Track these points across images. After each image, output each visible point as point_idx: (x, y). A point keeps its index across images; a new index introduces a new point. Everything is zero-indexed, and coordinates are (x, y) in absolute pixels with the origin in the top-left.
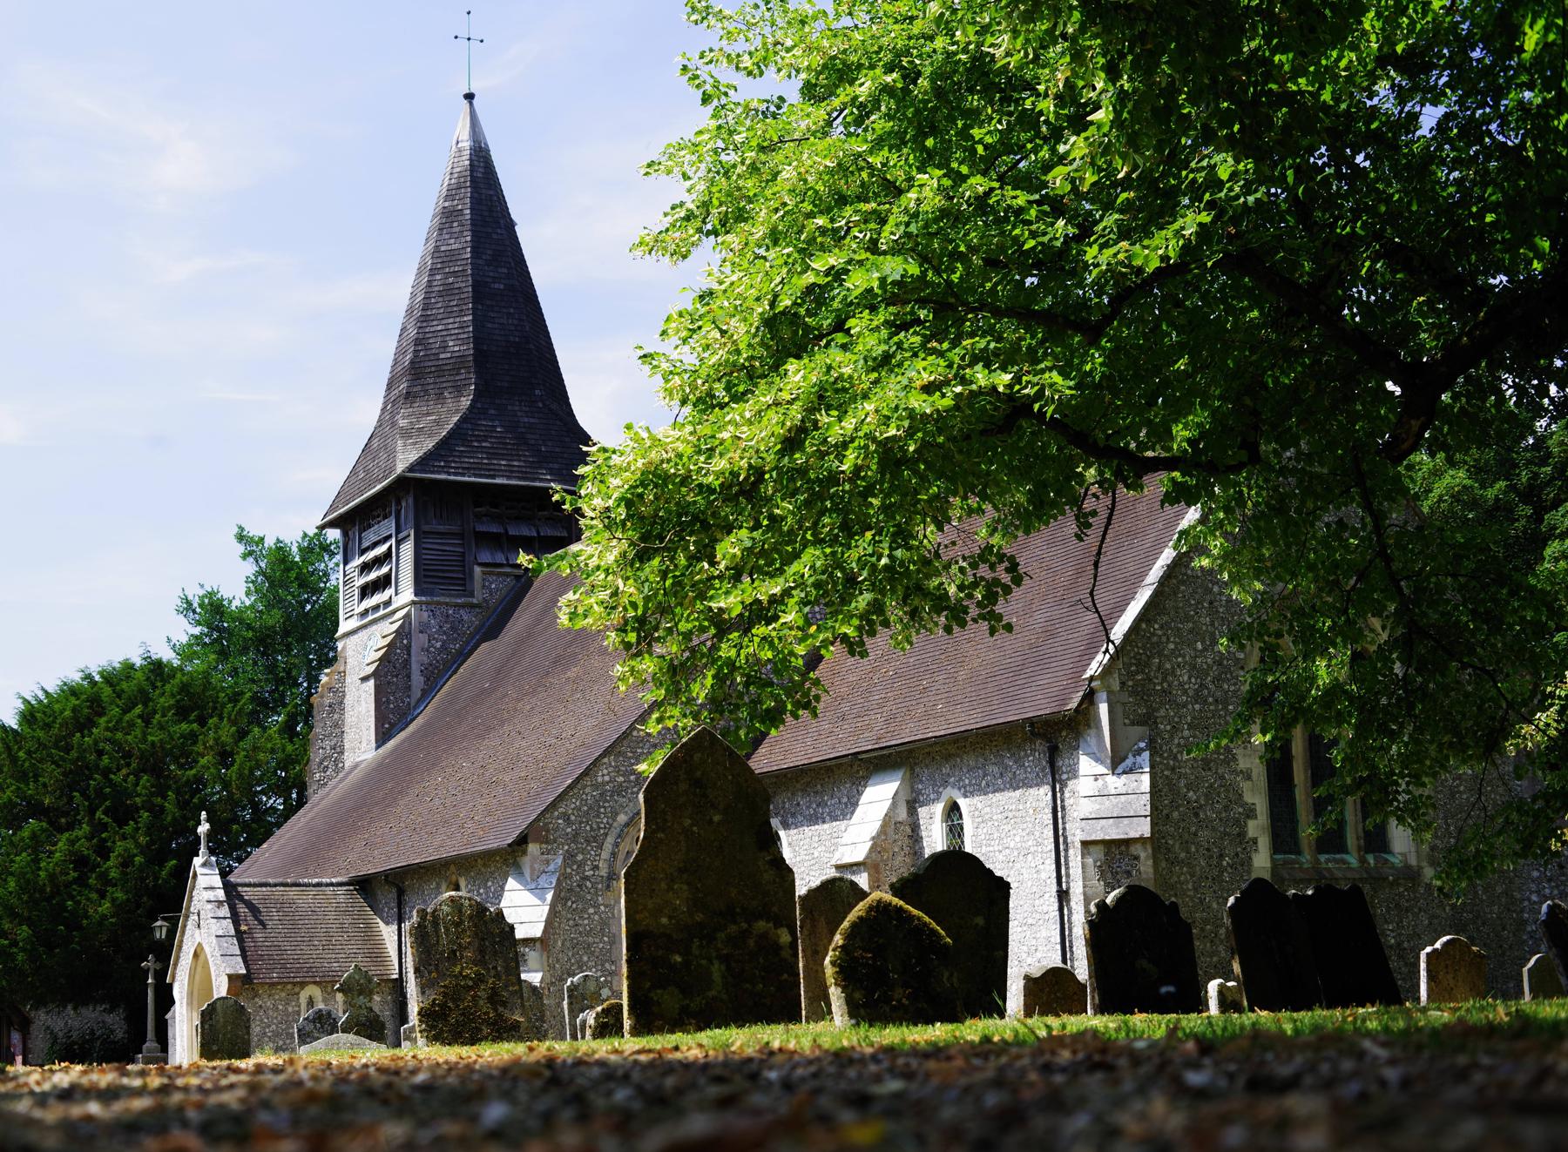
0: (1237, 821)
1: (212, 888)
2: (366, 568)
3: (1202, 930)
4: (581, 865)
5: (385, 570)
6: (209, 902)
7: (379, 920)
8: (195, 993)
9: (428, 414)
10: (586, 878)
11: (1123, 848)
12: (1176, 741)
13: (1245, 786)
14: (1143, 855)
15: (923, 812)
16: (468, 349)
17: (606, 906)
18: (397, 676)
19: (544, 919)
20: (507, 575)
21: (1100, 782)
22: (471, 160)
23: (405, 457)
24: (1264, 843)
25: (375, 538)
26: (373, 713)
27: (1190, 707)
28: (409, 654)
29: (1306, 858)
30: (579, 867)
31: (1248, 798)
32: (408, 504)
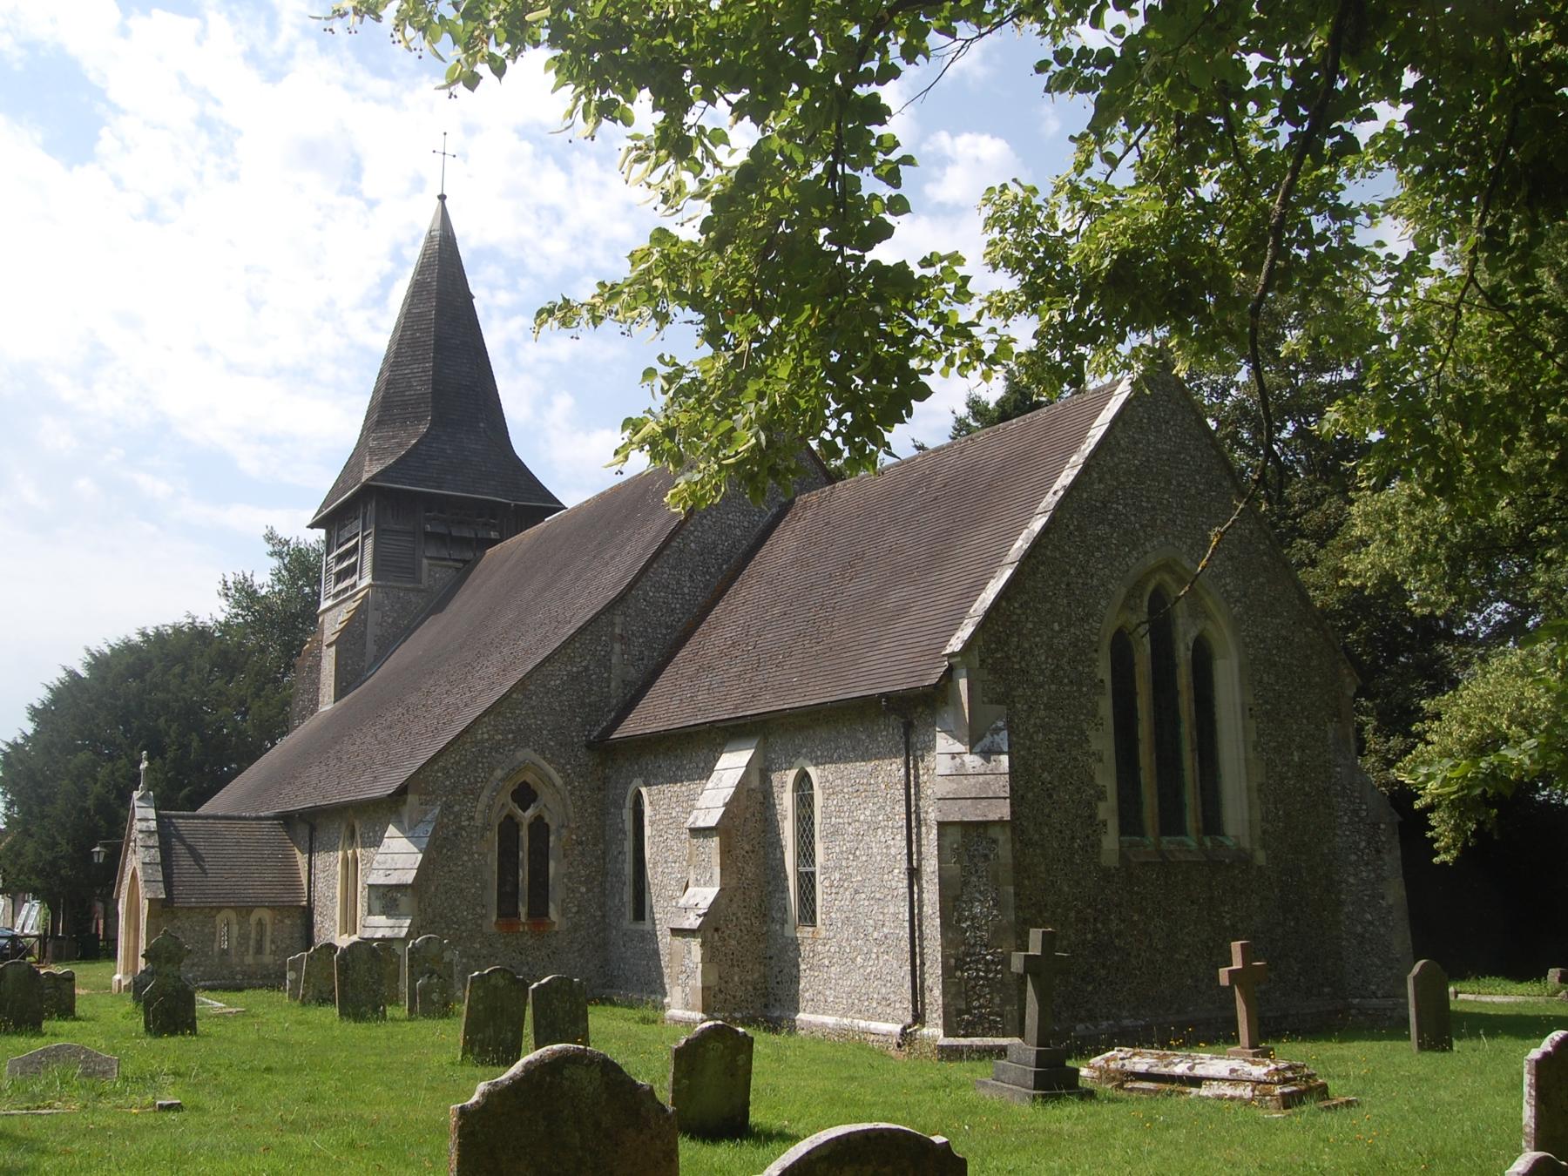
0: (1090, 803)
1: (147, 820)
2: (340, 558)
3: (1053, 913)
4: (458, 815)
5: (353, 559)
6: (141, 832)
7: (297, 851)
9: (393, 438)
10: (463, 828)
11: (981, 830)
12: (1032, 721)
13: (1097, 768)
14: (1001, 839)
15: (775, 777)
16: (426, 389)
17: (480, 855)
19: (416, 866)
20: (450, 567)
21: (958, 760)
22: (439, 245)
23: (370, 470)
24: (1113, 825)
25: (348, 536)
26: (333, 673)
27: (1046, 687)
28: (365, 628)
29: (1150, 839)
30: (455, 818)
31: (1099, 781)
32: (372, 507)
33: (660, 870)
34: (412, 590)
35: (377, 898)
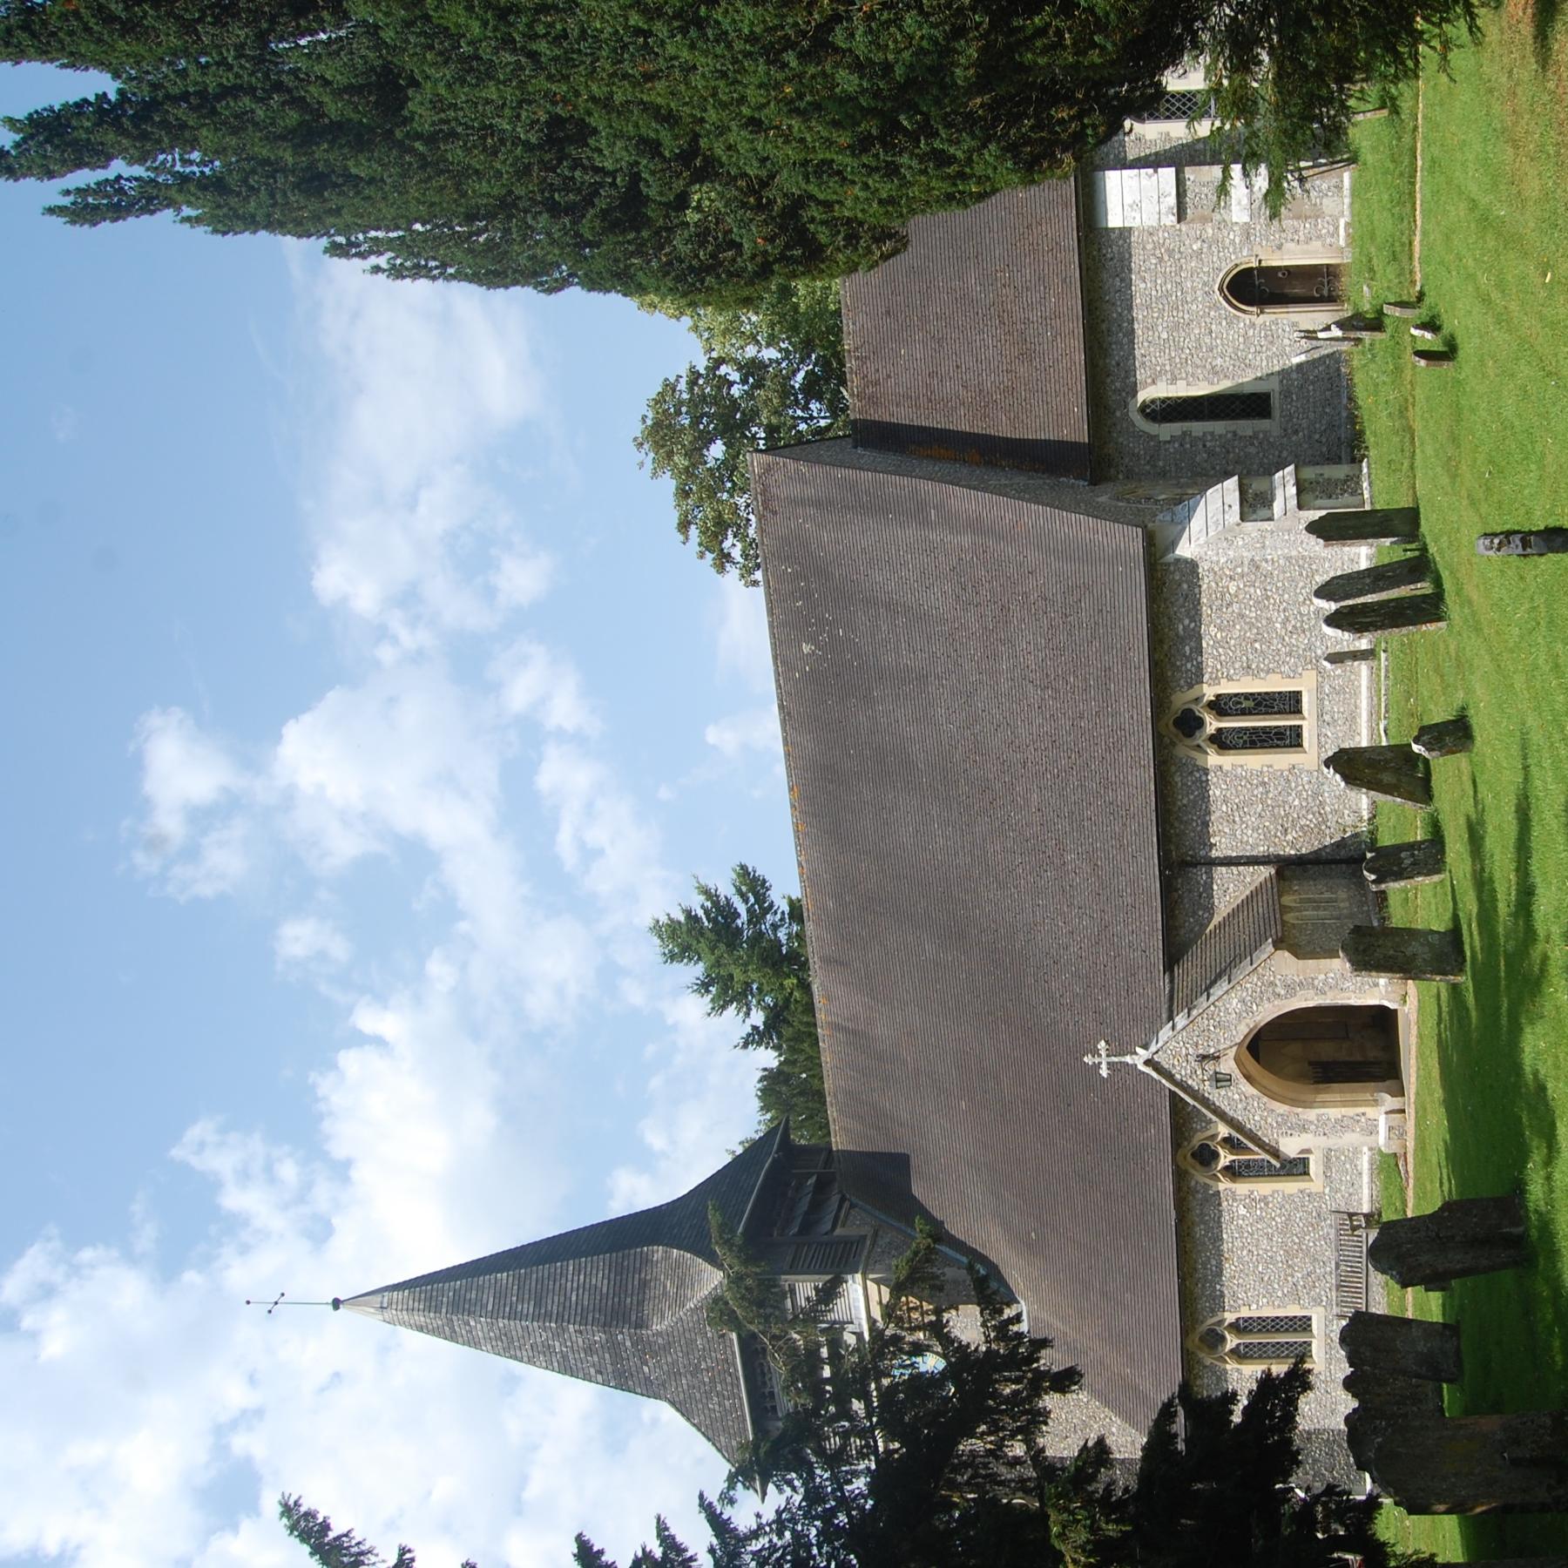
20: (846, 1216)
33: (1219, 361)
34: (874, 1243)
35: (1254, 512)
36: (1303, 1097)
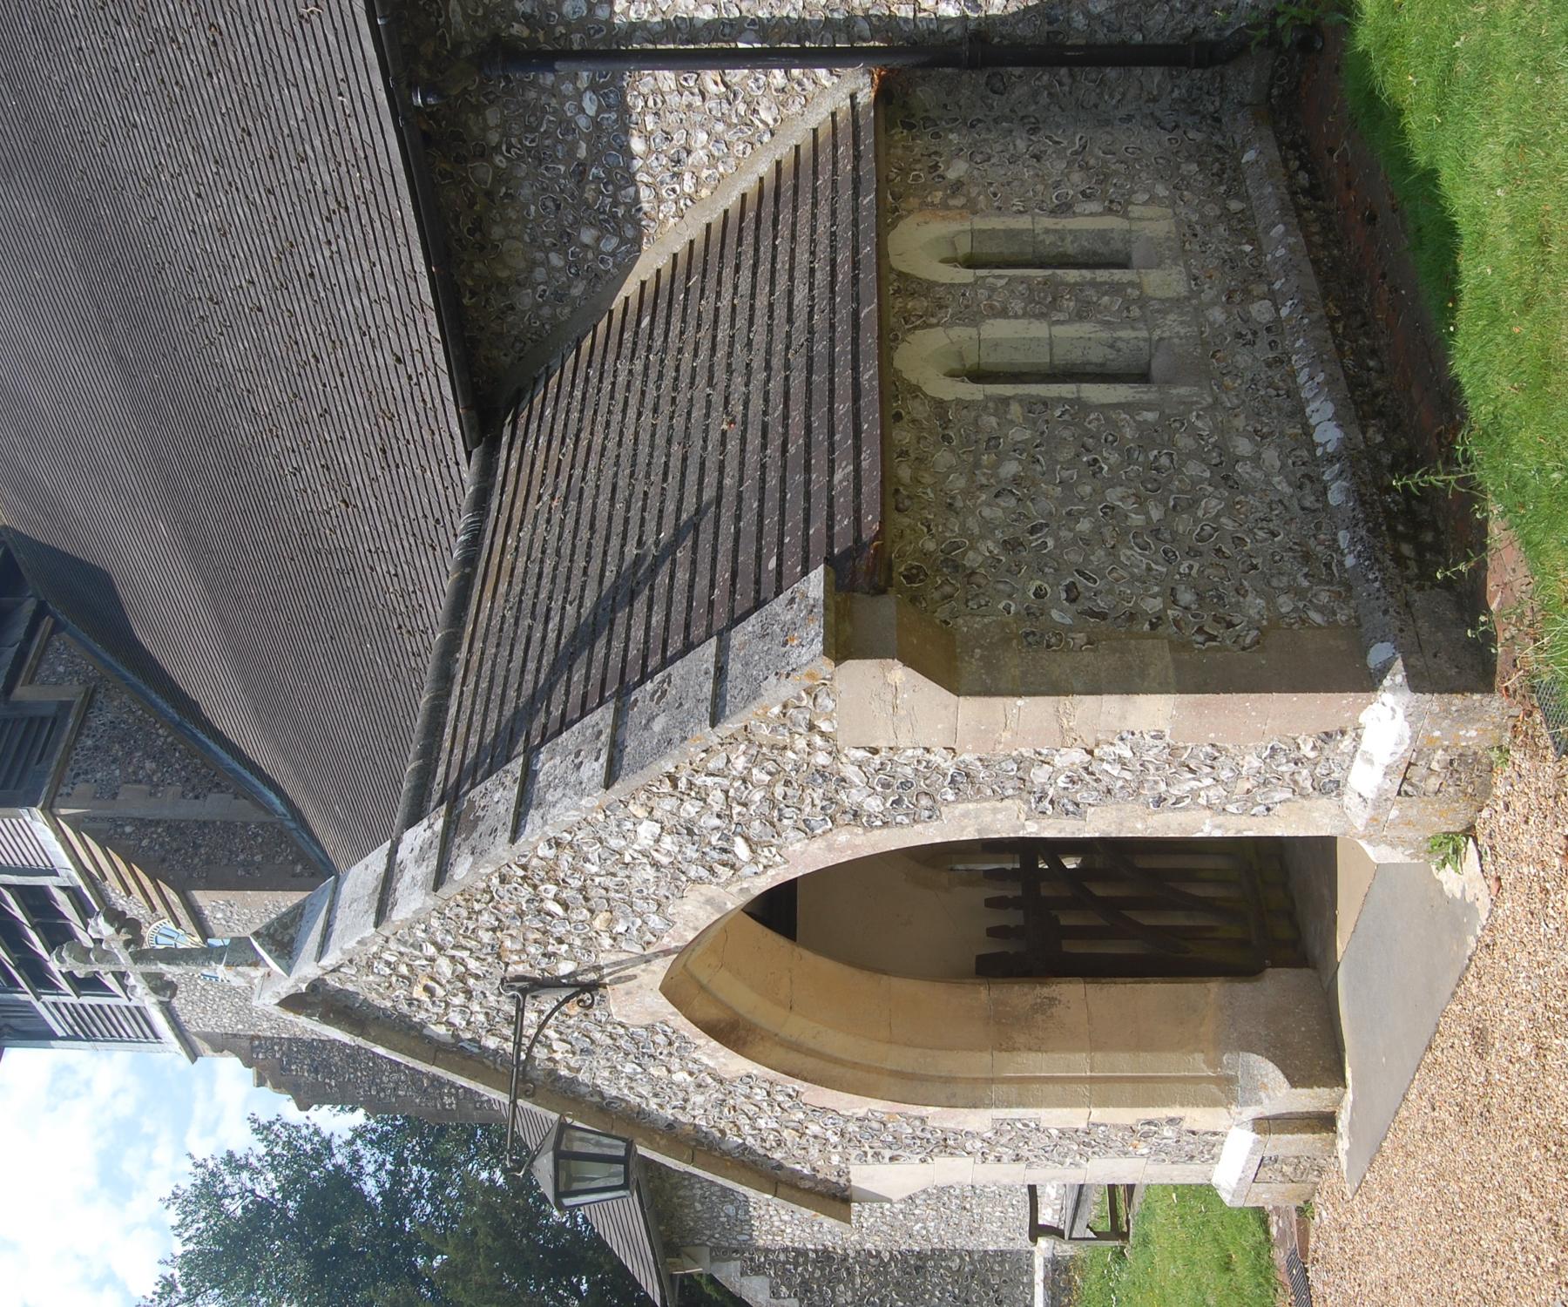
6: (440, 878)
7: (630, 288)
8: (905, 1059)
18: (196, 847)
28: (158, 823)
36: (949, 1063)
